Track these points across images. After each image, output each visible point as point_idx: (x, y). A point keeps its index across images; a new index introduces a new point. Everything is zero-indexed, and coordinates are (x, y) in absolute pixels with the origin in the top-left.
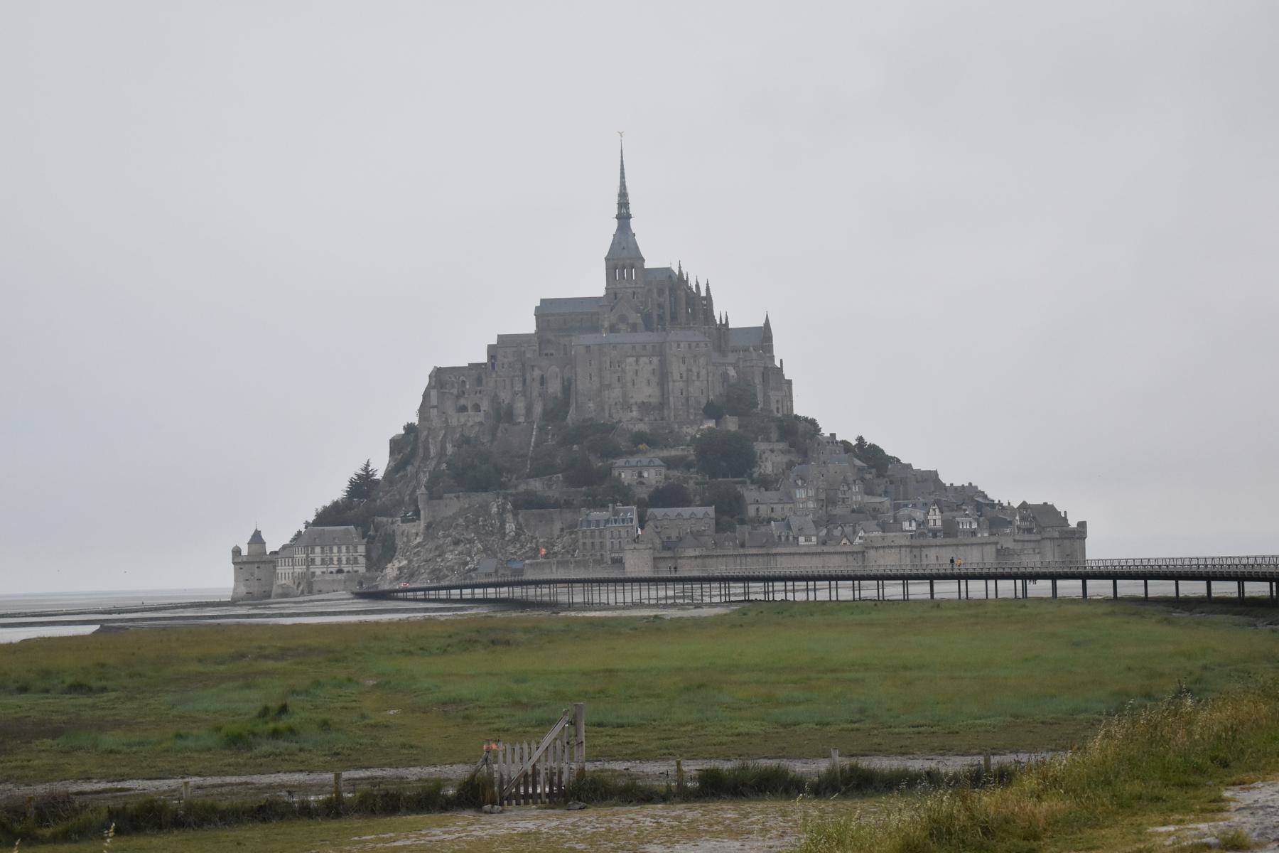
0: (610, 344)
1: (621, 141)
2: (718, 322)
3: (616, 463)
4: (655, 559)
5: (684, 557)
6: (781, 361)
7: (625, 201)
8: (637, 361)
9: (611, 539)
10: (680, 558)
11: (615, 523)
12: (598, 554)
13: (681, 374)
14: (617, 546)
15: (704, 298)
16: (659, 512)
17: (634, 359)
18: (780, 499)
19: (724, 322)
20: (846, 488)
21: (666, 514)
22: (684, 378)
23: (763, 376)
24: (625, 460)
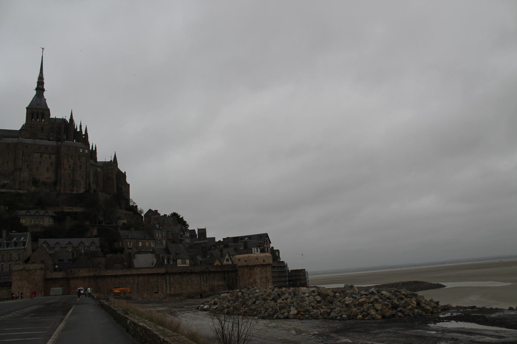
1: (43, 52)
2: (91, 149)
3: (19, 212)
4: (46, 280)
5: (77, 278)
6: (125, 172)
7: (42, 81)
8: (41, 156)
13: (70, 166)
15: (84, 135)
16: (52, 241)
17: (40, 154)
18: (145, 237)
19: (94, 149)
20: (182, 233)
21: (57, 243)
24: (26, 211)
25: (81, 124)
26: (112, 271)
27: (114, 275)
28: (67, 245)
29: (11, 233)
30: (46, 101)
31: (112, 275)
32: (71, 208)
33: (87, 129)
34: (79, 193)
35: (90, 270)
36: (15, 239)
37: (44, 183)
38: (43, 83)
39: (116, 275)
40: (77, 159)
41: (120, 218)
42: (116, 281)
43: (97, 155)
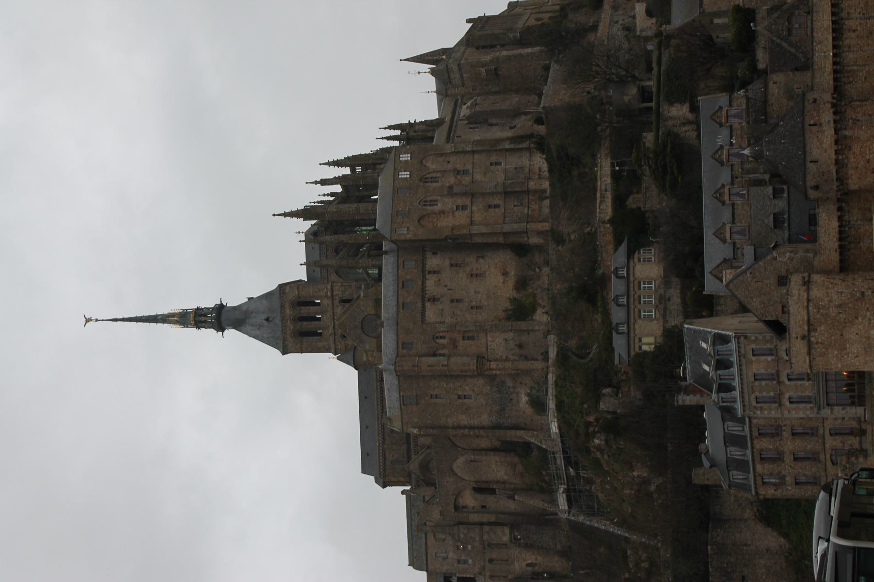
0: (397, 357)
2: (396, 143)
3: (619, 354)
4: (845, 266)
5: (840, 164)
6: (468, 21)
7: (192, 315)
8: (434, 300)
9: (780, 405)
10: (841, 180)
11: (734, 389)
12: (830, 442)
14: (807, 389)
15: (353, 170)
17: (428, 305)
19: (397, 132)
21: (719, 234)
22: (467, 201)
23: (484, 47)
25: (316, 183)
26: (819, 46)
27: (834, 39)
28: (723, 203)
29: (685, 379)
30: (255, 295)
31: (834, 47)
32: (598, 195)
33: (331, 160)
34: (550, 171)
35: (812, 122)
36: (706, 368)
37: (522, 284)
38: (198, 309)
39: (834, 30)
40: (435, 184)
41: (629, 29)
42: (854, 31)
43: (417, 121)
